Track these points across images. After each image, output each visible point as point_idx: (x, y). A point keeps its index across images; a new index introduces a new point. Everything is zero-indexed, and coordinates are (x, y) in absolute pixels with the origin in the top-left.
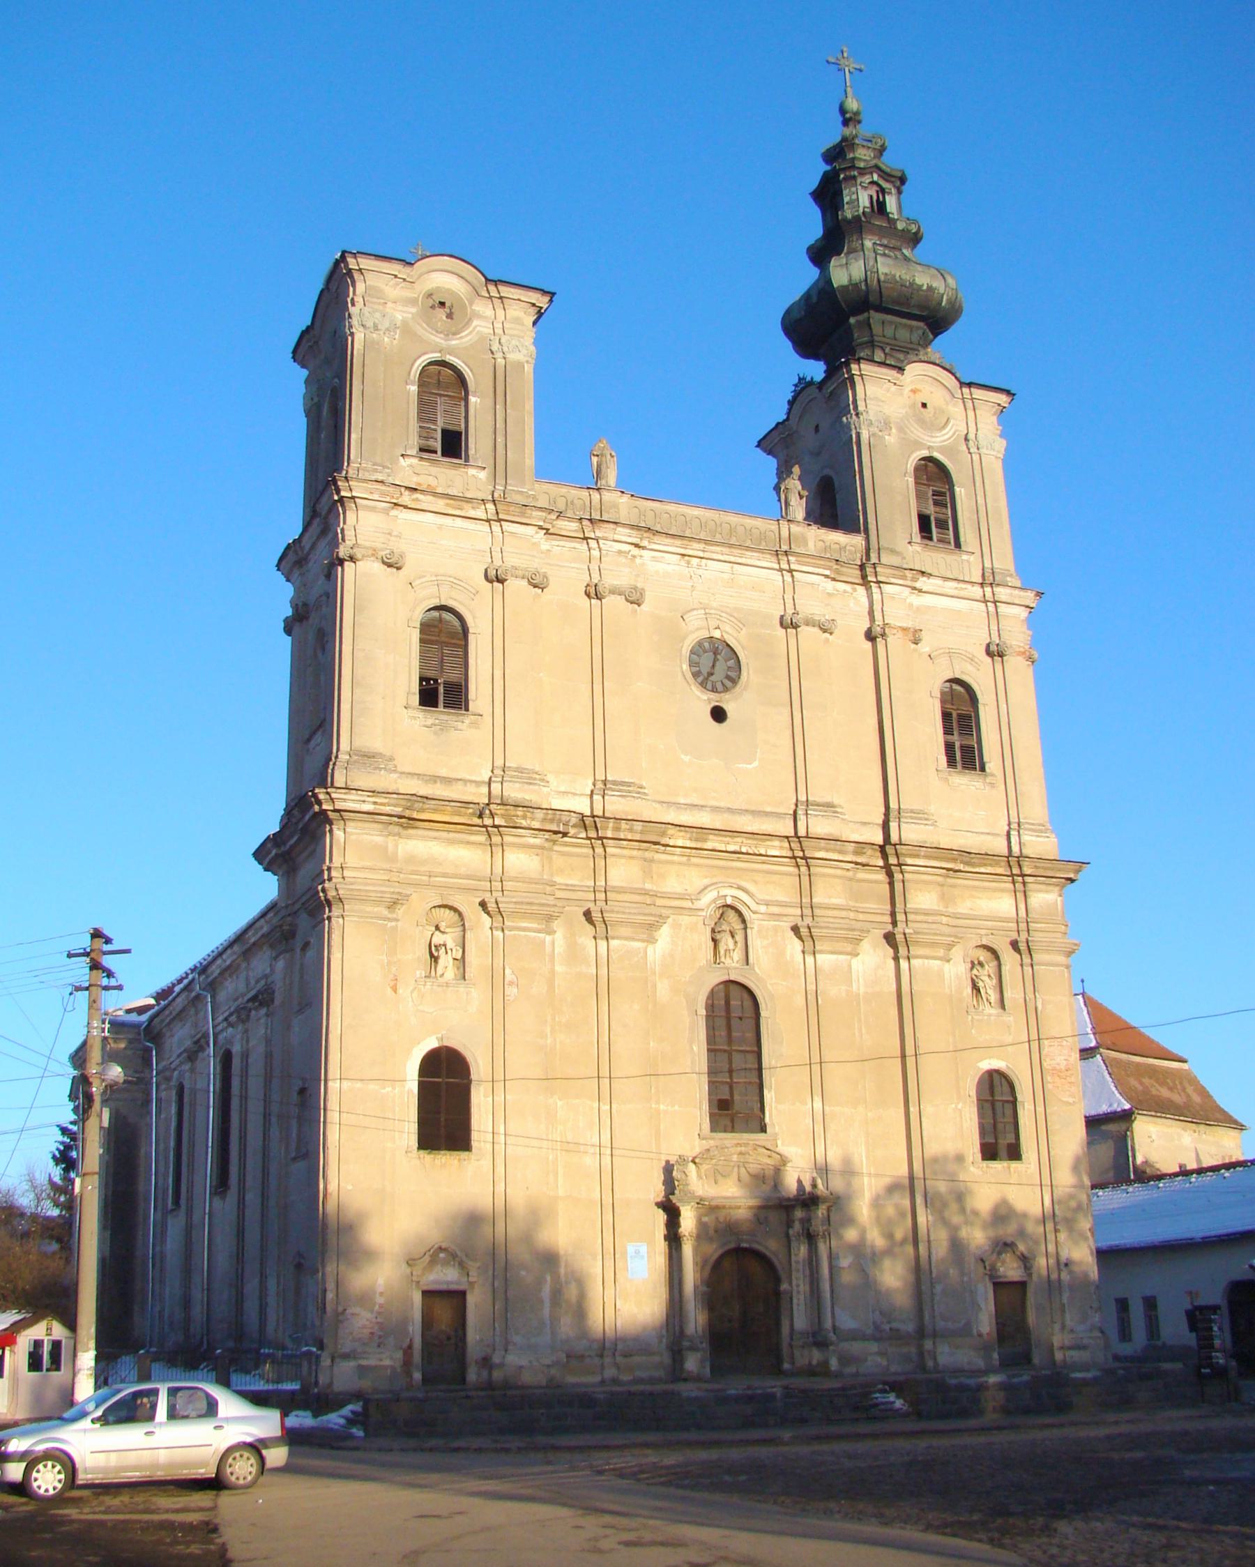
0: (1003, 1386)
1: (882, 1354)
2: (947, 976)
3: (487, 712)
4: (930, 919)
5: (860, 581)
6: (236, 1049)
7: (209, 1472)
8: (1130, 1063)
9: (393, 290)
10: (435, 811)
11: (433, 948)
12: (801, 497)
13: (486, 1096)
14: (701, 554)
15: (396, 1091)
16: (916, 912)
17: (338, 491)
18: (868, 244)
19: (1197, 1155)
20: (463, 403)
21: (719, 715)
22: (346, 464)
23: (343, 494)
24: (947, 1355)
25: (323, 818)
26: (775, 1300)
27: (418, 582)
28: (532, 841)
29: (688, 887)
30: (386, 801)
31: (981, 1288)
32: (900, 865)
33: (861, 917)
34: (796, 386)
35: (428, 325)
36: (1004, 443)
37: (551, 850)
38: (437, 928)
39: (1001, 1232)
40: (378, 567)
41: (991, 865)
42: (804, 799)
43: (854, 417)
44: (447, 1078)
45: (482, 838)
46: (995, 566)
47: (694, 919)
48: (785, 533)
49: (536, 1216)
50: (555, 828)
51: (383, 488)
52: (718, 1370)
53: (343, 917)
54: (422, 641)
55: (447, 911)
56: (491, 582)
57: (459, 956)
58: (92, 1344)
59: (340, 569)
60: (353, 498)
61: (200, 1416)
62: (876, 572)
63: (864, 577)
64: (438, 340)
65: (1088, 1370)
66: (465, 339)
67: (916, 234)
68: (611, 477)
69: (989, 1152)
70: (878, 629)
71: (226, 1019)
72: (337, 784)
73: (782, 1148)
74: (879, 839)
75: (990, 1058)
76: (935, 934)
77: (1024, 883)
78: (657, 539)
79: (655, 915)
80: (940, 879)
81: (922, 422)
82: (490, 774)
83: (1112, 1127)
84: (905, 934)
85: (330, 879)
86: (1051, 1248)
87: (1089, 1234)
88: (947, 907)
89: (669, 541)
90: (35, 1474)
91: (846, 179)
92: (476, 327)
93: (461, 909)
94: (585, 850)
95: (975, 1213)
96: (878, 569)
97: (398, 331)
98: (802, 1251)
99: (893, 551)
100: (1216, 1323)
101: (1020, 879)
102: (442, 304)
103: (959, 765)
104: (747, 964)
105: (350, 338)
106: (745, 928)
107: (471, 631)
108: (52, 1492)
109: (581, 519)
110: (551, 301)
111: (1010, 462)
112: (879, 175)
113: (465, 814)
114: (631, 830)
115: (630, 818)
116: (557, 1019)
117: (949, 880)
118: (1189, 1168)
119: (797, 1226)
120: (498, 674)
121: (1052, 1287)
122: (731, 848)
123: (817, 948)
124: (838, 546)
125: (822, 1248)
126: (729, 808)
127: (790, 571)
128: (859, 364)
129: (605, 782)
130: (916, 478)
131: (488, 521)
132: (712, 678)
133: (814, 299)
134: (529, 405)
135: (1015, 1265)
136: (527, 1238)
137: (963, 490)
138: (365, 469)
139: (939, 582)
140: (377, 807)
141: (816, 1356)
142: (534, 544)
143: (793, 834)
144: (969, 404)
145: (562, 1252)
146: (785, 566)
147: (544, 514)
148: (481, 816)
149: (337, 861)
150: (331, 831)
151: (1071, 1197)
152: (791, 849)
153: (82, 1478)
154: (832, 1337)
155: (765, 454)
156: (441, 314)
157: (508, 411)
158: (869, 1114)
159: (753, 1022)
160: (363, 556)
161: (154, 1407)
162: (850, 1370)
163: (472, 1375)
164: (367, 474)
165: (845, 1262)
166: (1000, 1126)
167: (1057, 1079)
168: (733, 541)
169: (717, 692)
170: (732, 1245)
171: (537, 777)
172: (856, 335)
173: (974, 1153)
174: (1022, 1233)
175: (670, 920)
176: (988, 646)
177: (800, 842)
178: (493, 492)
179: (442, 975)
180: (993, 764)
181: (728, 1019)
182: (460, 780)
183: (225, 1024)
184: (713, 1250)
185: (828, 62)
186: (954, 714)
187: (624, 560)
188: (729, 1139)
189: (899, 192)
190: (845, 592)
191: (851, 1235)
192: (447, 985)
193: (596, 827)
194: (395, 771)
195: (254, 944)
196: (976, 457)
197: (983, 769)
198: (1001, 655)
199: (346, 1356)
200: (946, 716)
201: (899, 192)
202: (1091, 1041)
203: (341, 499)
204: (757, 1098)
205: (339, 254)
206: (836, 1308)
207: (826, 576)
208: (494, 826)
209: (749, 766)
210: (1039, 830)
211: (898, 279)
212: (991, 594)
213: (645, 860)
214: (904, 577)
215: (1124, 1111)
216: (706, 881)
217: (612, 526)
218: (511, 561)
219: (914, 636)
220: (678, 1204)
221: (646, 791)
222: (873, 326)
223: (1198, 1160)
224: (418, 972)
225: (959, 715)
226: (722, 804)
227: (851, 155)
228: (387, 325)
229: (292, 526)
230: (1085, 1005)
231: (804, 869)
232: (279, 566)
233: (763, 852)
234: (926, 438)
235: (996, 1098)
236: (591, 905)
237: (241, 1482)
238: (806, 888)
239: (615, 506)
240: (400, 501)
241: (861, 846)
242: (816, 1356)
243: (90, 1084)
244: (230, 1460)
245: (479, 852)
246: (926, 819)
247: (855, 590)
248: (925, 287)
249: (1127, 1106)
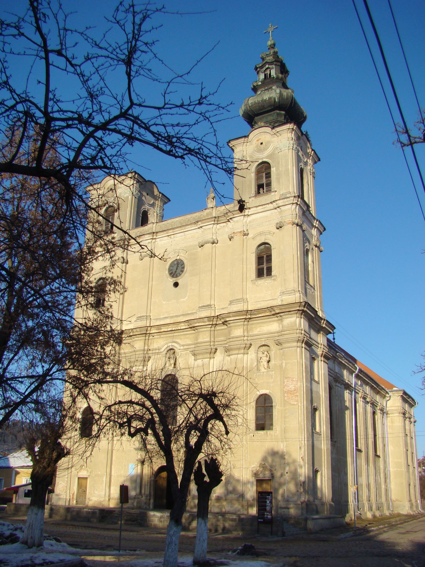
4: (238, 339)
14: (173, 233)
21: (176, 285)
41: (263, 313)
78: (158, 234)
89: (163, 233)
100: (268, 500)
114: (137, 331)
122: (169, 330)
139: (255, 209)
167: (289, 395)
190: (224, 226)
211: (256, 102)
226: (174, 315)
233: (179, 328)
234: (260, 155)
247: (227, 224)
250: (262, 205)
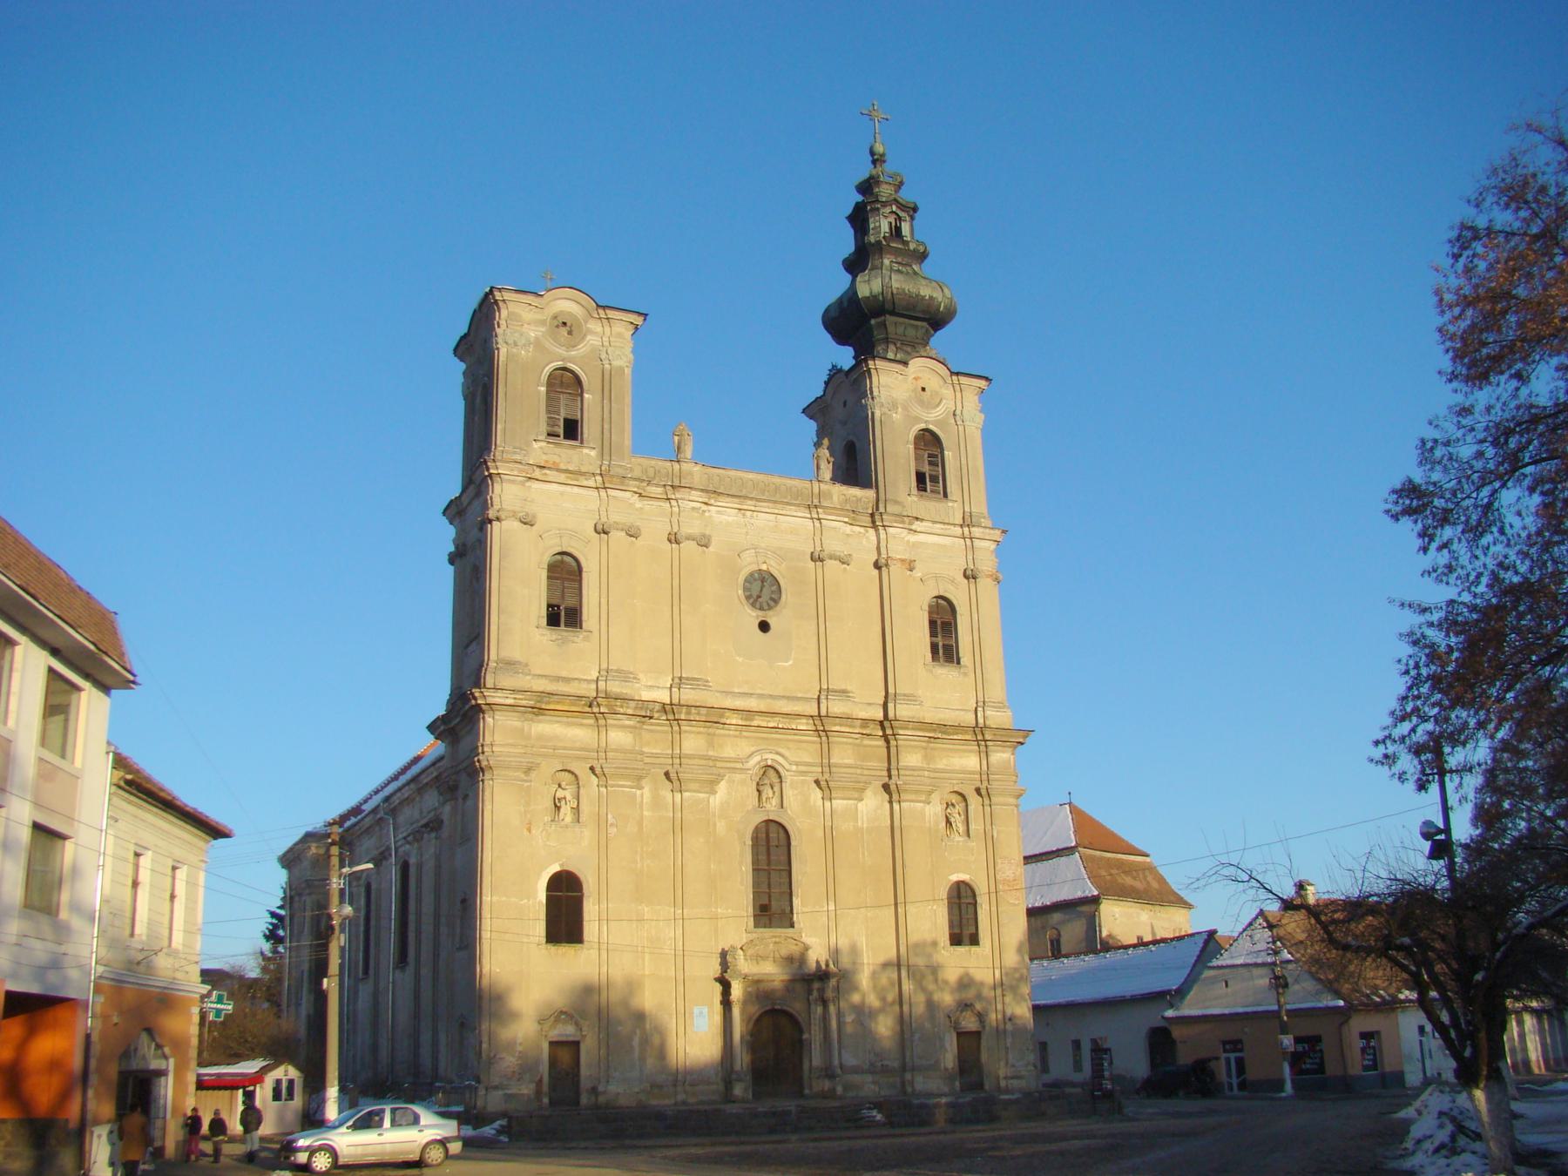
0: (949, 1105)
1: (874, 1083)
2: (927, 814)
3: (595, 628)
4: (916, 773)
5: (871, 525)
7: (415, 1157)
8: (1102, 858)
9: (527, 315)
10: (558, 703)
11: (557, 801)
12: (829, 463)
13: (594, 904)
14: (753, 508)
15: (531, 902)
16: (907, 768)
17: (488, 469)
18: (886, 262)
19: (1152, 928)
20: (579, 398)
21: (764, 627)
22: (493, 447)
23: (492, 471)
24: (921, 1083)
25: (478, 709)
26: (799, 1046)
27: (546, 534)
28: (627, 722)
30: (521, 697)
31: (947, 1037)
32: (894, 735)
33: (866, 772)
34: (830, 370)
35: (553, 339)
36: (983, 416)
37: (641, 728)
38: (560, 786)
39: (964, 996)
40: (517, 524)
42: (826, 687)
43: (870, 400)
44: (568, 891)
45: (592, 721)
46: (973, 510)
47: (743, 776)
48: (816, 490)
49: (632, 986)
50: (644, 714)
51: (520, 466)
52: (757, 1096)
53: (492, 779)
54: (549, 577)
55: (567, 773)
56: (599, 533)
57: (575, 806)
58: (336, 1082)
59: (489, 526)
60: (499, 474)
61: (408, 1125)
62: (882, 519)
63: (873, 522)
64: (560, 351)
65: (1013, 1094)
66: (582, 350)
67: (924, 252)
68: (688, 451)
69: (956, 940)
70: (883, 561)
72: (488, 686)
73: (805, 939)
74: (880, 715)
75: (958, 872)
76: (919, 785)
77: (986, 746)
79: (716, 775)
80: (924, 744)
81: (921, 403)
82: (598, 674)
83: (1085, 909)
84: (897, 785)
85: (483, 753)
86: (999, 1007)
87: (1027, 997)
88: (929, 764)
89: (729, 499)
90: (314, 1159)
91: (872, 210)
92: (588, 342)
93: (577, 772)
94: (666, 728)
95: (946, 982)
96: (884, 517)
97: (532, 346)
98: (819, 1010)
99: (896, 502)
101: (983, 743)
102: (564, 324)
103: (941, 660)
104: (782, 807)
105: (496, 352)
106: (781, 782)
107: (584, 570)
108: (324, 1169)
109: (665, 485)
110: (645, 319)
111: (985, 431)
112: (897, 207)
113: (579, 706)
114: (698, 714)
115: (698, 704)
116: (645, 849)
117: (932, 745)
118: (1145, 940)
119: (815, 994)
120: (604, 601)
121: (1000, 1033)
123: (833, 795)
124: (854, 499)
125: (832, 1009)
126: (771, 695)
127: (819, 519)
128: (874, 360)
129: (680, 678)
130: (915, 444)
131: (597, 488)
132: (760, 600)
133: (845, 304)
134: (628, 400)
135: (973, 1019)
136: (625, 1003)
137: (950, 453)
138: (507, 452)
139: (930, 524)
140: (517, 701)
141: (827, 1084)
142: (631, 504)
143: (817, 714)
144: (957, 388)
145: (647, 1014)
146: (815, 516)
147: (637, 483)
148: (590, 706)
149: (488, 740)
150: (484, 718)
151: (1016, 969)
152: (815, 725)
153: (341, 1161)
154: (839, 1071)
156: (564, 331)
157: (613, 405)
158: (869, 914)
159: (785, 848)
160: (506, 517)
161: (382, 1120)
162: (851, 1094)
163: (584, 1100)
164: (509, 456)
165: (849, 1019)
166: (964, 921)
168: (777, 498)
169: (763, 610)
170: (769, 1008)
171: (632, 676)
172: (875, 333)
173: (944, 941)
174: (979, 997)
175: (726, 778)
176: (965, 570)
177: (821, 720)
178: (601, 466)
179: (563, 820)
180: (966, 658)
181: (768, 849)
182: (576, 679)
184: (755, 1010)
185: (862, 114)
186: (939, 622)
187: (696, 514)
188: (767, 933)
189: (912, 218)
190: (860, 533)
191: (856, 998)
192: (567, 826)
193: (673, 712)
194: (529, 674)
195: (427, 784)
196: (961, 428)
197: (958, 663)
198: (974, 578)
199: (496, 1088)
200: (932, 623)
201: (912, 218)
202: (1071, 842)
203: (490, 475)
204: (788, 903)
205: (489, 289)
206: (843, 1051)
207: (846, 522)
208: (600, 713)
209: (786, 664)
210: (999, 706)
211: (907, 292)
212: (968, 533)
213: (709, 734)
214: (903, 522)
215: (1093, 896)
216: (753, 749)
217: (688, 490)
218: (615, 517)
219: (910, 565)
220: (730, 979)
221: (710, 684)
222: (888, 326)
223: (1153, 933)
224: (546, 818)
225: (943, 623)
227: (877, 190)
228: (523, 342)
229: (455, 490)
230: (1071, 812)
231: (824, 739)
235: (962, 901)
236: (670, 768)
237: (434, 1162)
238: (826, 752)
239: (691, 474)
240: (533, 476)
241: (865, 722)
242: (827, 1084)
243: (332, 919)
244: (428, 1150)
245: (590, 731)
246: (915, 701)
247: (867, 531)
248: (927, 297)
249: (1096, 893)
250: (944, 523)
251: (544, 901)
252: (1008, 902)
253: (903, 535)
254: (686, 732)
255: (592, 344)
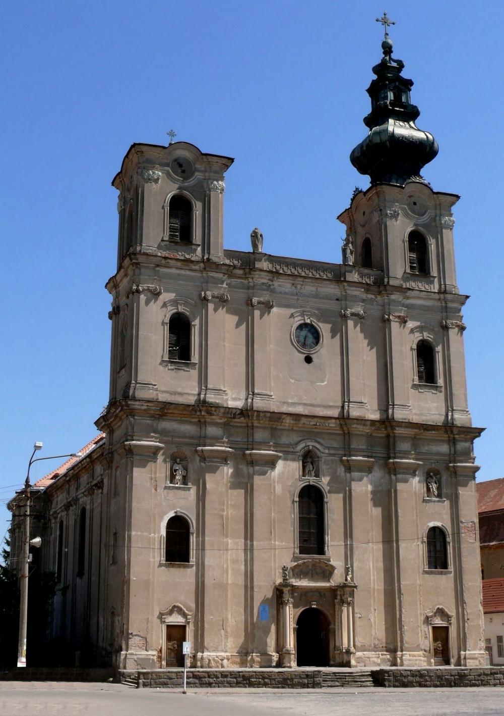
6: (88, 507)
15: (156, 535)
21: (308, 360)
29: (291, 442)
34: (354, 192)
71: (83, 493)
116: (229, 503)
133: (365, 148)
139: (418, 292)
155: (340, 223)
183: (82, 495)
209: (322, 384)
216: (300, 439)
221: (273, 397)
232: (106, 287)
251: (165, 535)
252: (468, 541)
253: (400, 300)
254: (257, 427)
255: (198, 178)
